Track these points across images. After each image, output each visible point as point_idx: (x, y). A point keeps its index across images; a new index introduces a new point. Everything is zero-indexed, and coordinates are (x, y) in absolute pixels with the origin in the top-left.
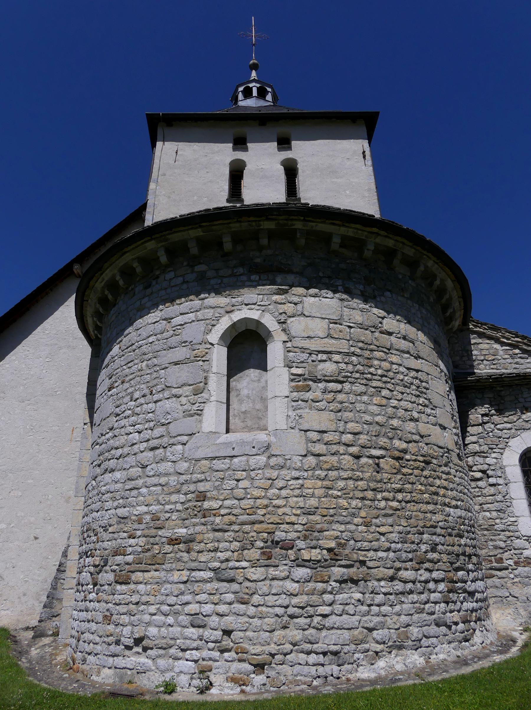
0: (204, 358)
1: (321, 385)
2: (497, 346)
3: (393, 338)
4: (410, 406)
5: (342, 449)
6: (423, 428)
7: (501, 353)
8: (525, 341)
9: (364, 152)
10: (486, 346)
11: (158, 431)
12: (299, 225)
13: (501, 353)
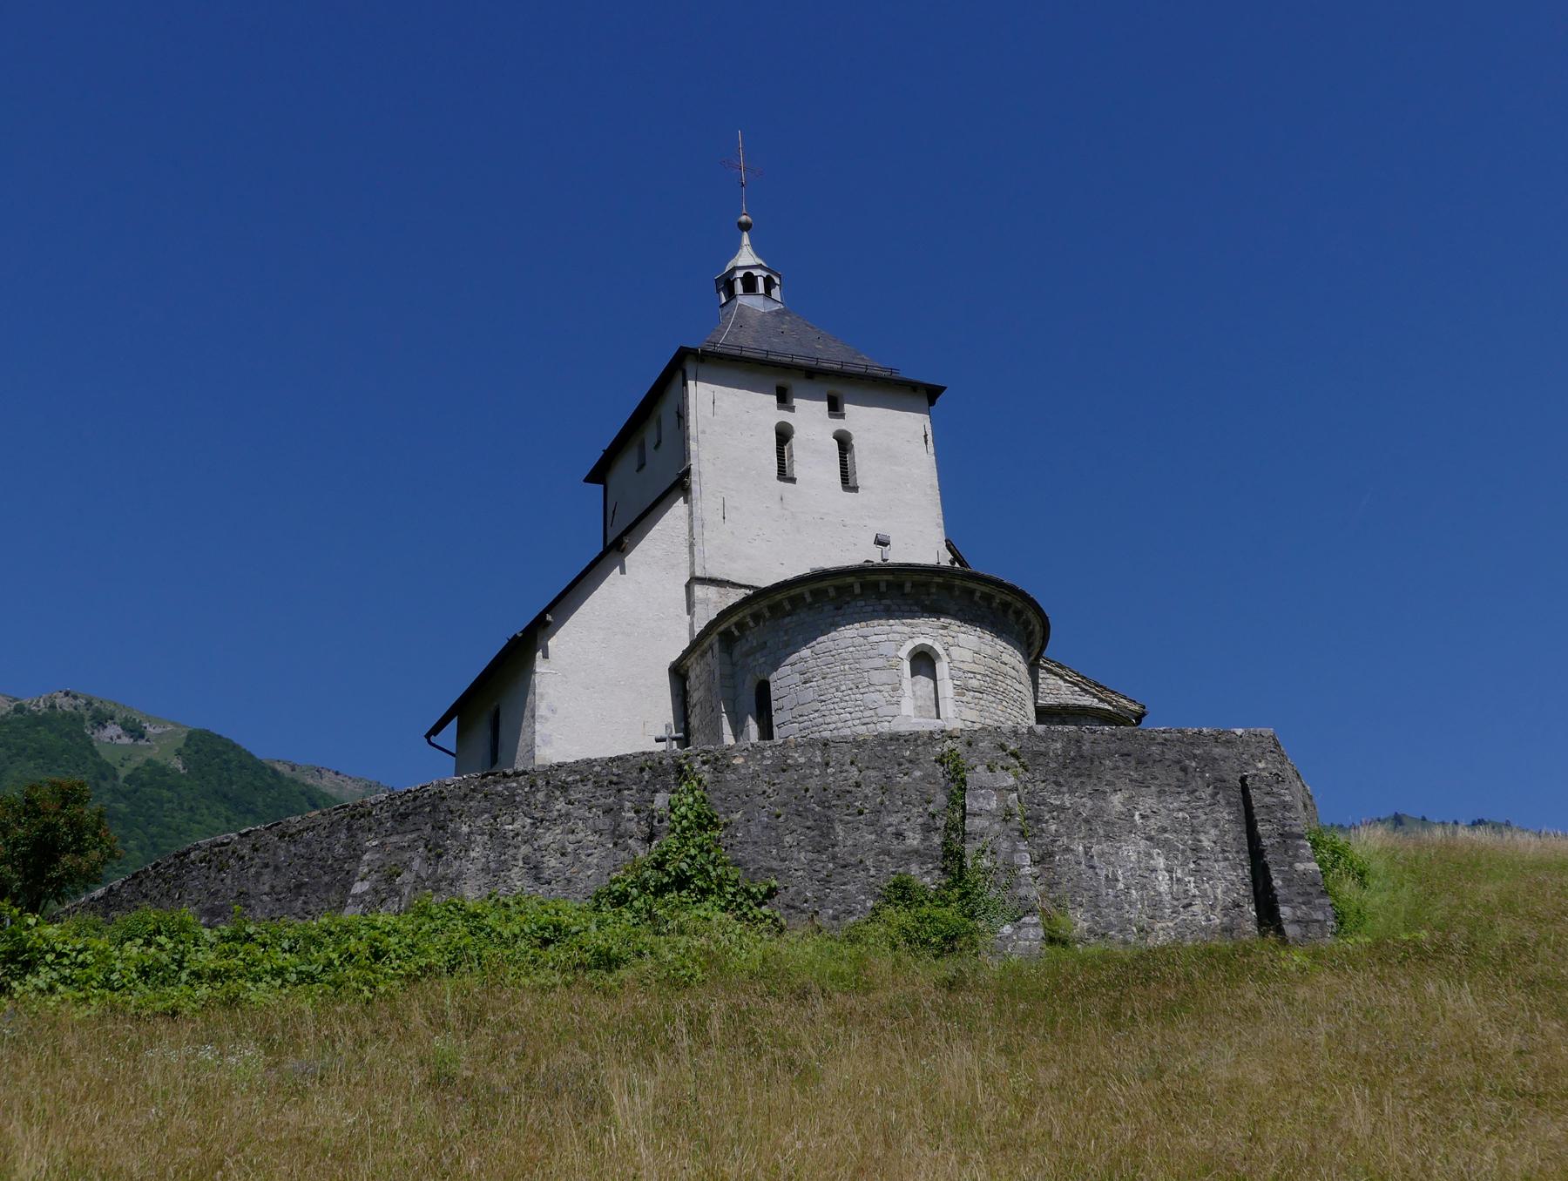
1: (972, 693)
2: (1061, 682)
3: (1007, 667)
4: (1017, 714)
8: (1084, 681)
9: (926, 436)
10: (1053, 682)
11: (867, 713)
12: (957, 582)
13: (1064, 689)
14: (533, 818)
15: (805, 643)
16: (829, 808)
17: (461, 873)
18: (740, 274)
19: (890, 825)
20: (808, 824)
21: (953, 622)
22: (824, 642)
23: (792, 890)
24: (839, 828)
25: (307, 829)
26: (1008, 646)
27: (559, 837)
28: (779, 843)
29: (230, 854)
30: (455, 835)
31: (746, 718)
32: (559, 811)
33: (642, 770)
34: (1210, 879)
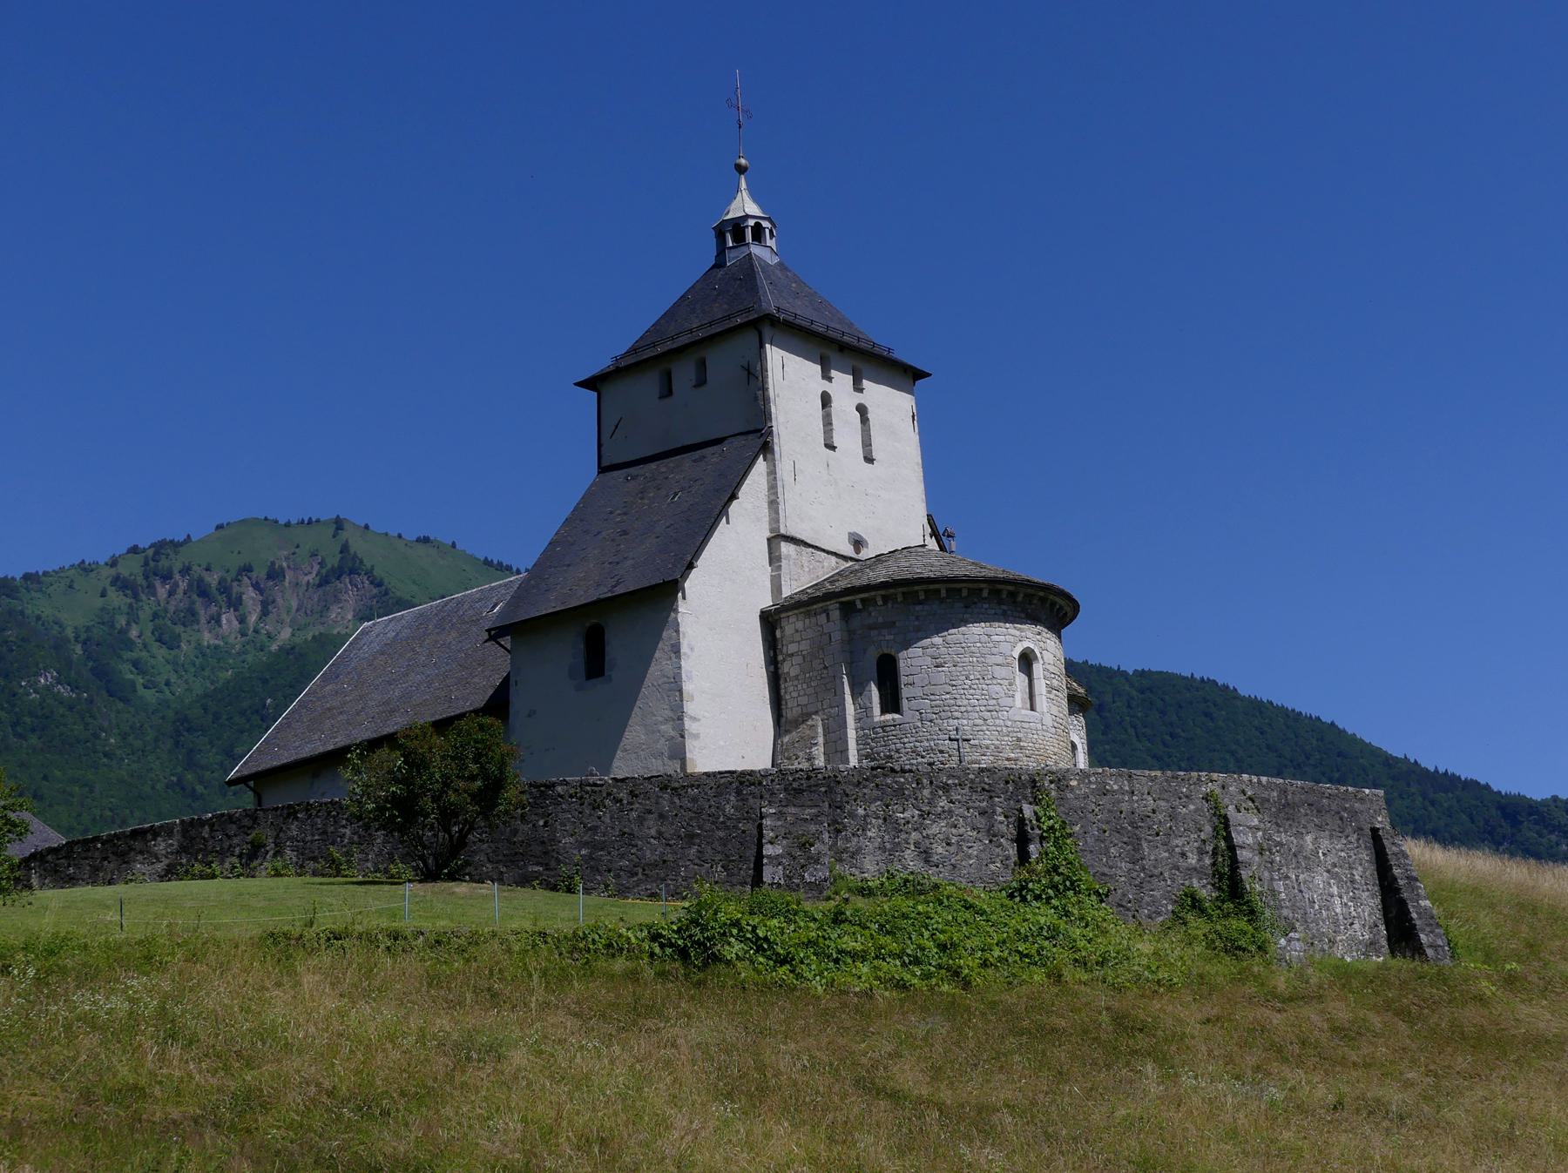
14: (920, 810)
15: (937, 632)
16: (1137, 828)
17: (860, 849)
18: (751, 222)
19: (1177, 846)
20: (1125, 839)
22: (955, 634)
23: (1119, 891)
24: (1145, 845)
25: (693, 786)
27: (944, 829)
28: (1107, 853)
29: (605, 795)
30: (852, 815)
31: (868, 682)
32: (943, 807)
33: (1007, 782)
34: (1361, 905)
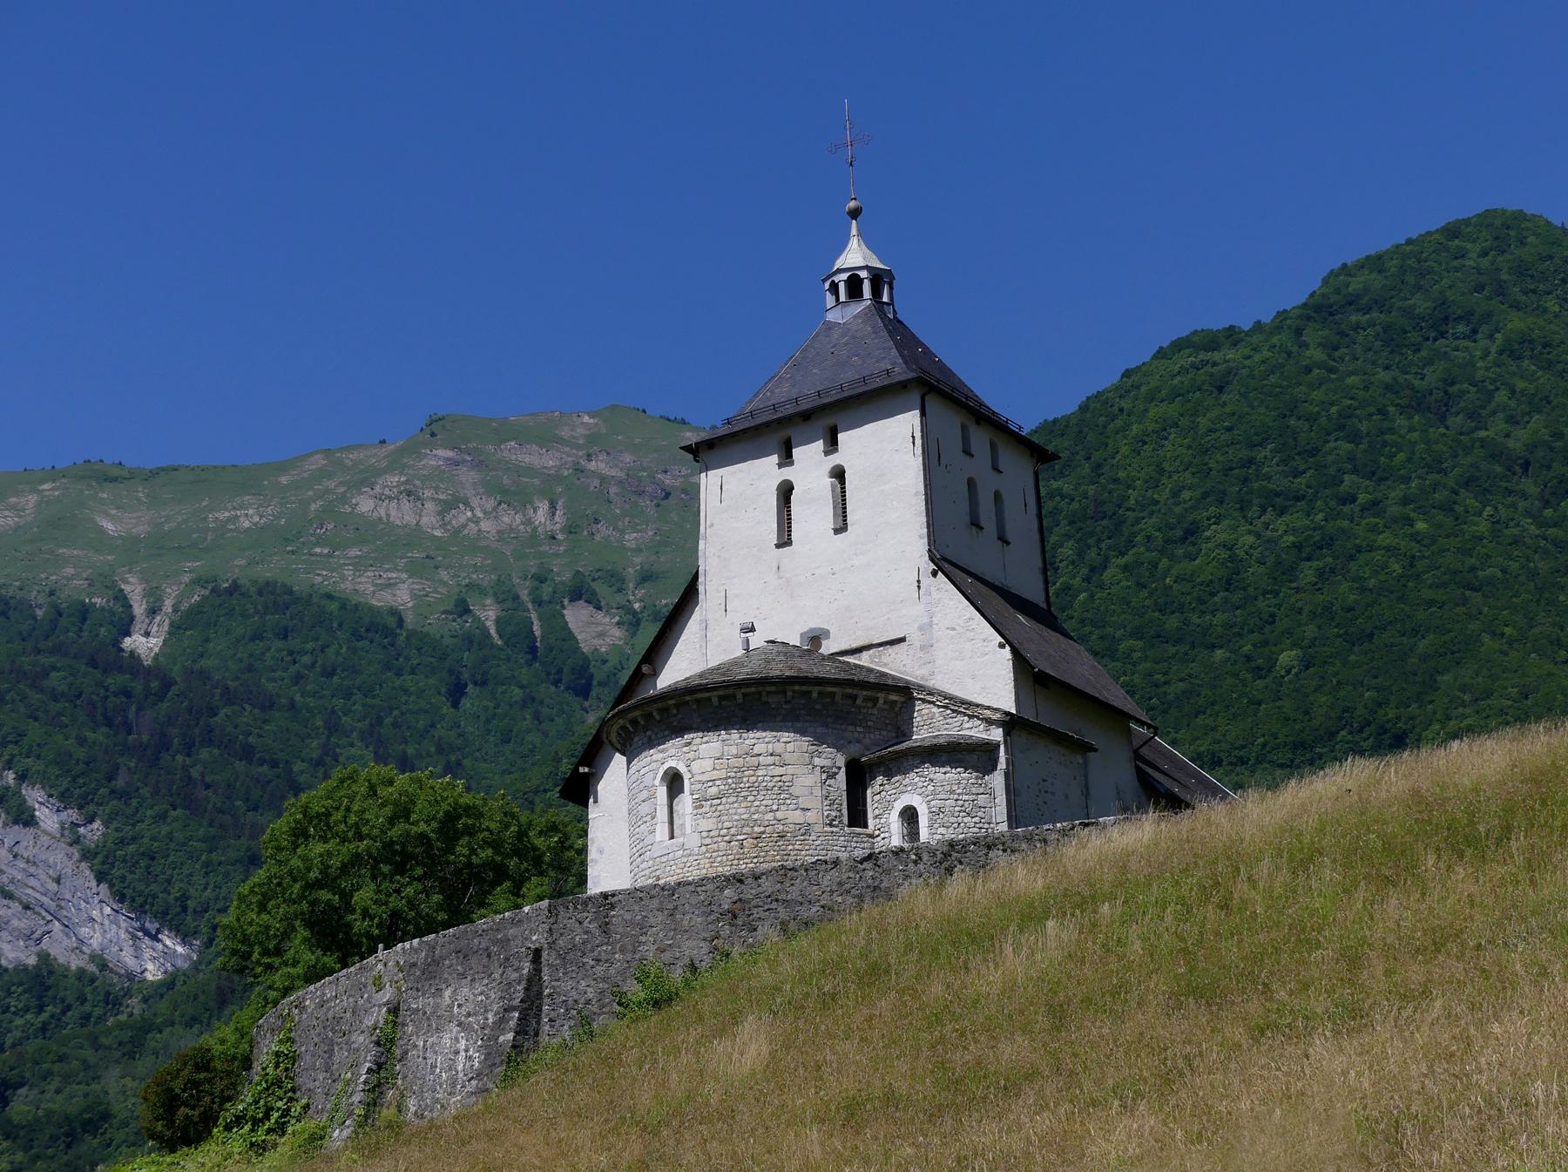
0: (653, 796)
2: (935, 710)
4: (770, 802)
5: (720, 839)
6: (779, 815)
7: (937, 715)
10: (927, 711)
12: (688, 698)
21: (695, 735)
26: (764, 734)
